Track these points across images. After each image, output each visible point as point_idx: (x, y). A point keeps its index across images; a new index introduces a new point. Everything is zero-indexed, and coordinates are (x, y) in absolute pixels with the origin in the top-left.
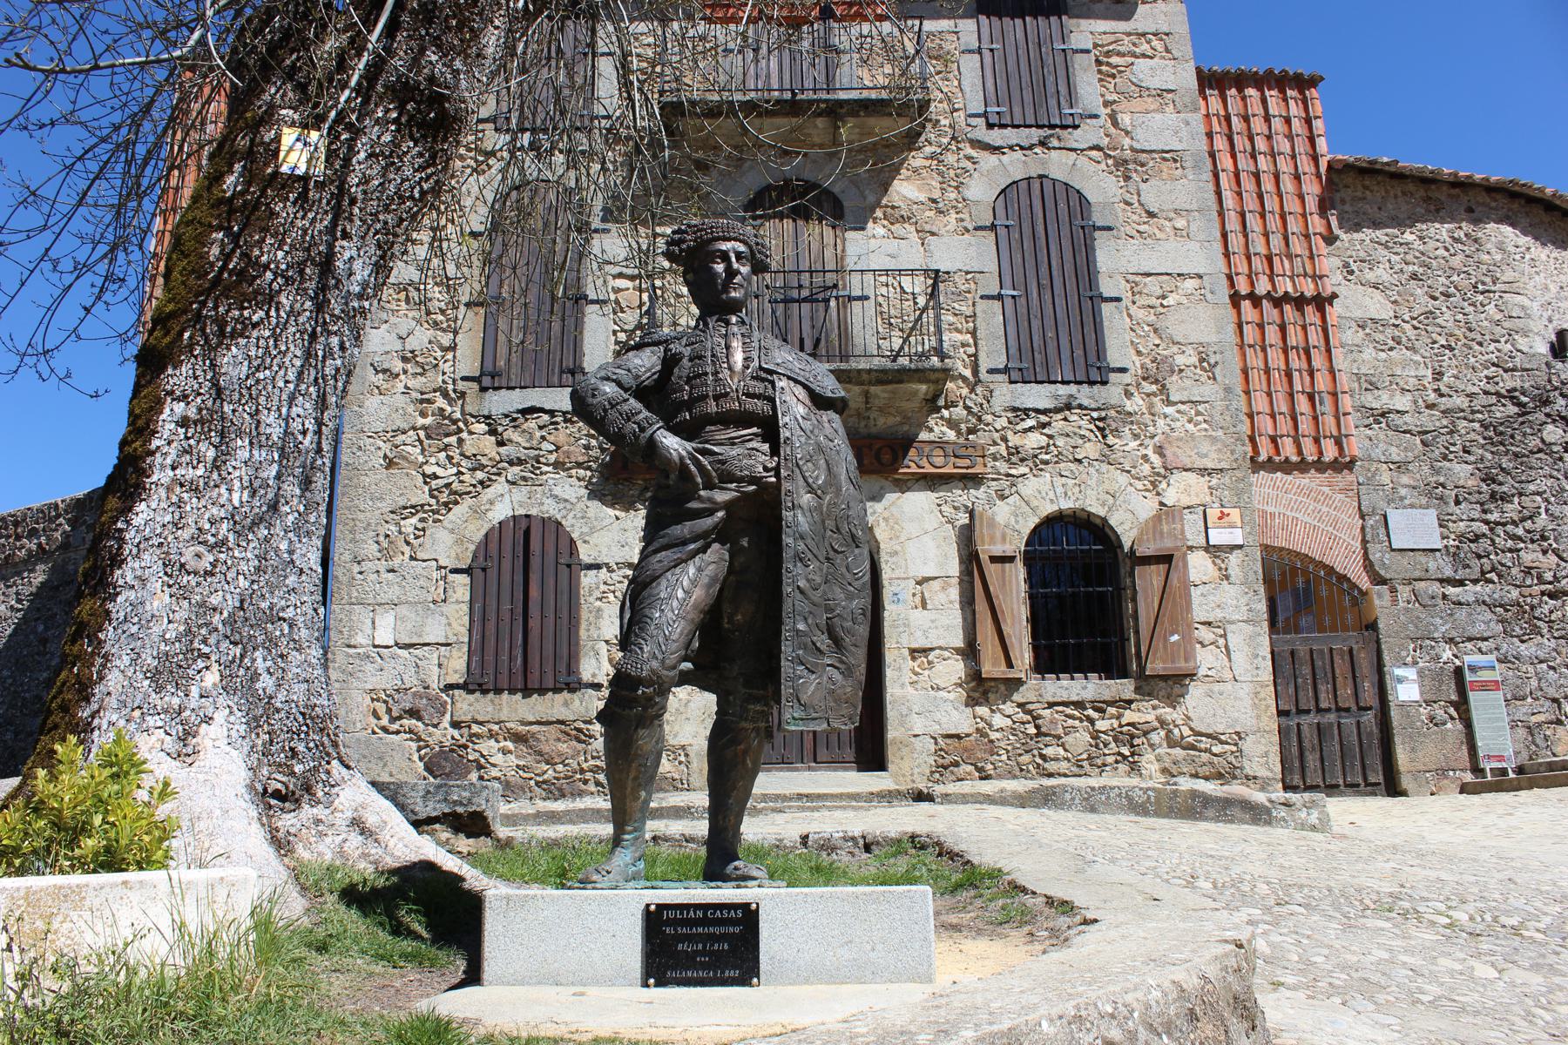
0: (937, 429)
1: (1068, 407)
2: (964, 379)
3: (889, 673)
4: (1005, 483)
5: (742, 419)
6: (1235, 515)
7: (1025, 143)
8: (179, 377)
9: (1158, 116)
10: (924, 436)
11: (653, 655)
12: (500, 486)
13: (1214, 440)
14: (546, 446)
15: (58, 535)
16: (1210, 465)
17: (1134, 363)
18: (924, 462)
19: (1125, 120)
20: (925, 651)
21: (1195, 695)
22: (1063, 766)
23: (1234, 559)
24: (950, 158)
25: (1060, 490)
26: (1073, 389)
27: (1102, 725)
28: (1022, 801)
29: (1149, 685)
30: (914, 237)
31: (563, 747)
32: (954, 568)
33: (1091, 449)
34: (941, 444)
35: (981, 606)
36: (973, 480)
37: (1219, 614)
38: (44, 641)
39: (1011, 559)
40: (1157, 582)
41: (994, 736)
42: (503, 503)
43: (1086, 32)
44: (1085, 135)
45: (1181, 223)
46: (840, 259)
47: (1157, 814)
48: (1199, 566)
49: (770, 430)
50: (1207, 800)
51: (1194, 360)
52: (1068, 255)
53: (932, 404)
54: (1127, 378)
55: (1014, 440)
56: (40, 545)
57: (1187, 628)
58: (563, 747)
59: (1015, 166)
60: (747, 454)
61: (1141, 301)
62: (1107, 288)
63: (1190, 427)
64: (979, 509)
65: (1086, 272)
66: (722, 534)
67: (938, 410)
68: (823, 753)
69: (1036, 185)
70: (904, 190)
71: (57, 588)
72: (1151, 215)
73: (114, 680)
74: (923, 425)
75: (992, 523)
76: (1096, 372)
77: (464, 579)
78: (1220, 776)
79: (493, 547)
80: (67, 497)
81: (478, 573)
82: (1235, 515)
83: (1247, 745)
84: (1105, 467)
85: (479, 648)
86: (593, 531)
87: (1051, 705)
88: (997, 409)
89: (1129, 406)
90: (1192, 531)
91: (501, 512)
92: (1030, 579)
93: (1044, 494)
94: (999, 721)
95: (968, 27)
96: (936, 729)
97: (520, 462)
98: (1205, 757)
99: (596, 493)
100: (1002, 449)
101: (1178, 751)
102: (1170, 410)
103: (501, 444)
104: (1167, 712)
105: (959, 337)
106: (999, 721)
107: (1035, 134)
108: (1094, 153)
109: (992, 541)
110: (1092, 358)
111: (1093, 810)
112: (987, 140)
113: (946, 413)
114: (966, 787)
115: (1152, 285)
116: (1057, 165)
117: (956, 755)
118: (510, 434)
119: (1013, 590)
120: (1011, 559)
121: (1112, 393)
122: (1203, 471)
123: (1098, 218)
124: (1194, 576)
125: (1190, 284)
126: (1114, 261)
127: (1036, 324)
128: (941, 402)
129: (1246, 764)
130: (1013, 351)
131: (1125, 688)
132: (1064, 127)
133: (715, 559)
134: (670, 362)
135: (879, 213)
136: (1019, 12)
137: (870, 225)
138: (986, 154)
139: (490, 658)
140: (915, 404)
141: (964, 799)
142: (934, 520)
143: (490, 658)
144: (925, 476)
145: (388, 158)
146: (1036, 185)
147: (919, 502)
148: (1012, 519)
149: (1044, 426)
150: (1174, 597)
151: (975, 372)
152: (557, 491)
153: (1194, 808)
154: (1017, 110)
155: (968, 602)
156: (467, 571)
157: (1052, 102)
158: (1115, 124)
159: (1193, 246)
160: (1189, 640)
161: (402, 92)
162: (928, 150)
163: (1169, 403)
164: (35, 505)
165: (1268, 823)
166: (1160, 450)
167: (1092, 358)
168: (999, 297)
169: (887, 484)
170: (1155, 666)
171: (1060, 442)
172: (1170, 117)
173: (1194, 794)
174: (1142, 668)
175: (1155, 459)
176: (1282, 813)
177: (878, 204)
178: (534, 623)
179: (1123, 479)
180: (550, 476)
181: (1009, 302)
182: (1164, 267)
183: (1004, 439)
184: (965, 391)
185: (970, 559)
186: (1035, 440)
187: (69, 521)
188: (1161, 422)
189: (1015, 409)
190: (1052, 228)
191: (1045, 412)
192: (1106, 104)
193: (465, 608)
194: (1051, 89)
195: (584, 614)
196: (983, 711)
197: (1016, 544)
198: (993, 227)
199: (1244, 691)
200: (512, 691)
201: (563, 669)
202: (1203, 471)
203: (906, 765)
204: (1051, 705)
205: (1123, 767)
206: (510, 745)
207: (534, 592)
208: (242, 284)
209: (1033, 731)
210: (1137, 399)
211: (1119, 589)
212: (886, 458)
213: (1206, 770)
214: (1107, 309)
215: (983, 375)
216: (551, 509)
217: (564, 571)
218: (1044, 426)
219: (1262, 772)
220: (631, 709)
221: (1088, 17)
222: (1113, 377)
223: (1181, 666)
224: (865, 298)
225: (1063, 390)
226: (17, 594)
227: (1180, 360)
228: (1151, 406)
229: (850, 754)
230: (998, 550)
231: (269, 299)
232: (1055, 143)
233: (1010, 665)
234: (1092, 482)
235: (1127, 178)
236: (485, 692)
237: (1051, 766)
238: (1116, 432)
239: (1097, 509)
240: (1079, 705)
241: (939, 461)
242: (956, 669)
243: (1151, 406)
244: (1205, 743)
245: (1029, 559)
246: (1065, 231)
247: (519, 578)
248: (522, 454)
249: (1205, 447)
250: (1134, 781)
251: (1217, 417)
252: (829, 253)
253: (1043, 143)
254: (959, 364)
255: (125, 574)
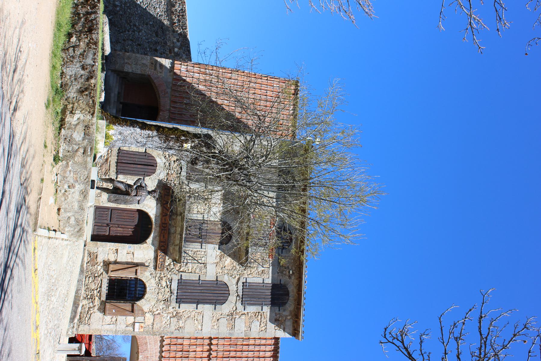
0: (168, 261)
1: (171, 293)
2: (180, 269)
3: (113, 244)
4: (154, 275)
5: (137, 193)
6: (142, 330)
7: (238, 291)
8: (155, 133)
9: (244, 326)
10: (167, 258)
11: (116, 183)
12: (164, 160)
13: (160, 328)
14: (173, 172)
15: (177, 29)
16: (154, 326)
17: (181, 311)
18: (161, 257)
19: (243, 317)
20: (117, 252)
21: (100, 315)
22: (87, 282)
23: (131, 329)
24: (235, 272)
25: (151, 288)
26: (176, 294)
27: (95, 292)
28: (82, 266)
29: (103, 304)
30: (216, 261)
31: (104, 169)
32: (136, 261)
33: (160, 297)
34: (164, 261)
35: (126, 266)
36: (155, 268)
37: (118, 323)
38: (147, 24)
39: (136, 274)
40: (127, 308)
41: (96, 266)
42: (160, 161)
43: (267, 310)
44: (240, 307)
45: (216, 327)
46: (212, 243)
47: (75, 296)
48: (130, 319)
49: (136, 196)
50: (77, 308)
51: (181, 326)
52: (209, 298)
53: (174, 260)
54: (177, 308)
55: (164, 279)
56: (175, 23)
57: (116, 315)
58: (104, 169)
59: (232, 288)
60: (133, 193)
61: (196, 314)
62: (199, 306)
63: (164, 322)
64: (149, 268)
65: (205, 302)
66: (126, 190)
67: (173, 262)
68: (96, 227)
69: (227, 292)
70: (228, 261)
71: (162, 28)
72: (218, 320)
73: (120, 127)
74: (170, 257)
75: (145, 271)
76: (179, 301)
77: (144, 151)
78: (80, 319)
79: (150, 158)
80: (188, 33)
81: (145, 154)
82: (142, 330)
83: (87, 326)
84: (156, 300)
85: (128, 153)
86: (152, 180)
87: (101, 280)
88: (172, 276)
89: (170, 308)
90: (139, 319)
91: (158, 160)
92: (131, 280)
93: (151, 284)
94: (99, 268)
95: (269, 281)
96: (99, 253)
97: (170, 165)
98: (85, 316)
99: (160, 182)
100: (162, 276)
101: (87, 309)
102: (169, 318)
103: (174, 161)
104: (97, 308)
105: (190, 269)
106: (99, 268)
107: (241, 294)
108: (235, 308)
109: (141, 270)
110: (182, 300)
111: (78, 281)
112: (240, 282)
113: (172, 263)
114: (86, 259)
115: (200, 318)
116: (232, 298)
117: (93, 257)
118: (176, 164)
119: (128, 274)
120: (136, 274)
121: (174, 304)
122: (153, 324)
123: (217, 306)
124: (128, 318)
125: (200, 327)
126: (207, 309)
127: (192, 288)
128: (175, 263)
129: (82, 325)
130: (186, 281)
131: (104, 298)
132: (242, 301)
133: (124, 190)
134: (143, 187)
135: (223, 253)
136: (272, 294)
137: (220, 251)
138: (236, 281)
139: (125, 155)
140: (175, 256)
141: (84, 253)
142: (147, 257)
143: (125, 155)
144: (157, 257)
145: (187, 156)
146: (227, 292)
147: (152, 255)
148: (146, 276)
149: (167, 286)
150: (123, 312)
151: (181, 272)
152: (162, 173)
153: (76, 304)
154: (247, 290)
155: (127, 263)
156: (146, 152)
157: (249, 299)
158: (242, 314)
159: (209, 330)
160: (114, 314)
161: (196, 158)
162: (238, 267)
163: (170, 318)
164: (187, 22)
165: (70, 322)
166: (159, 314)
167: (182, 300)
168: (199, 279)
169: (156, 248)
170: (108, 306)
171: (163, 290)
172: (244, 329)
173: (79, 305)
174: (108, 302)
175: (157, 312)
176: (72, 326)
177: (225, 253)
178: (132, 165)
179: (153, 304)
180: (166, 172)
181: (198, 282)
182: (203, 321)
183: (165, 277)
184: (177, 269)
185: (137, 265)
186: (164, 284)
187: (181, 33)
188: (166, 315)
189: (172, 280)
190: (216, 295)
191: (170, 287)
192: (248, 313)
193: (137, 151)
194: (252, 299)
195: (133, 177)
196: (102, 264)
197: (140, 276)
198: (217, 280)
199: (99, 327)
200: (117, 159)
201: (121, 171)
202: (153, 324)
203: (91, 245)
204: (101, 280)
205: (85, 296)
206: (105, 158)
207: (139, 166)
208: (167, 140)
209: (96, 275)
210: (172, 310)
211: (127, 301)
212: (163, 248)
213: (82, 315)
214: (195, 305)
215: (181, 273)
216: (158, 171)
217: (144, 173)
218: (167, 286)
219: (80, 329)
220: (111, 180)
221: (270, 311)
222: (178, 305)
223: (107, 312)
224: (201, 248)
225: (175, 292)
226: (162, 15)
227: (181, 322)
228: (170, 313)
229: (95, 233)
230: (139, 271)
231: (165, 142)
232: (238, 298)
233: (112, 271)
234: (152, 296)
235: (228, 315)
236: (118, 153)
237: (87, 279)
238: (164, 303)
239: (146, 297)
240: (101, 287)
241: (161, 260)
242: (112, 259)
243: (170, 313)
244: (88, 316)
245: (136, 279)
246: (215, 298)
247: (143, 163)
248: (171, 166)
249: (159, 325)
250: (82, 298)
251: (166, 329)
252: (214, 240)
253: (238, 295)
254: (183, 268)
255: (132, 128)
